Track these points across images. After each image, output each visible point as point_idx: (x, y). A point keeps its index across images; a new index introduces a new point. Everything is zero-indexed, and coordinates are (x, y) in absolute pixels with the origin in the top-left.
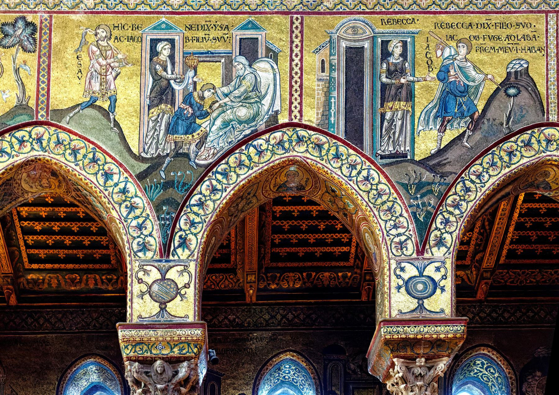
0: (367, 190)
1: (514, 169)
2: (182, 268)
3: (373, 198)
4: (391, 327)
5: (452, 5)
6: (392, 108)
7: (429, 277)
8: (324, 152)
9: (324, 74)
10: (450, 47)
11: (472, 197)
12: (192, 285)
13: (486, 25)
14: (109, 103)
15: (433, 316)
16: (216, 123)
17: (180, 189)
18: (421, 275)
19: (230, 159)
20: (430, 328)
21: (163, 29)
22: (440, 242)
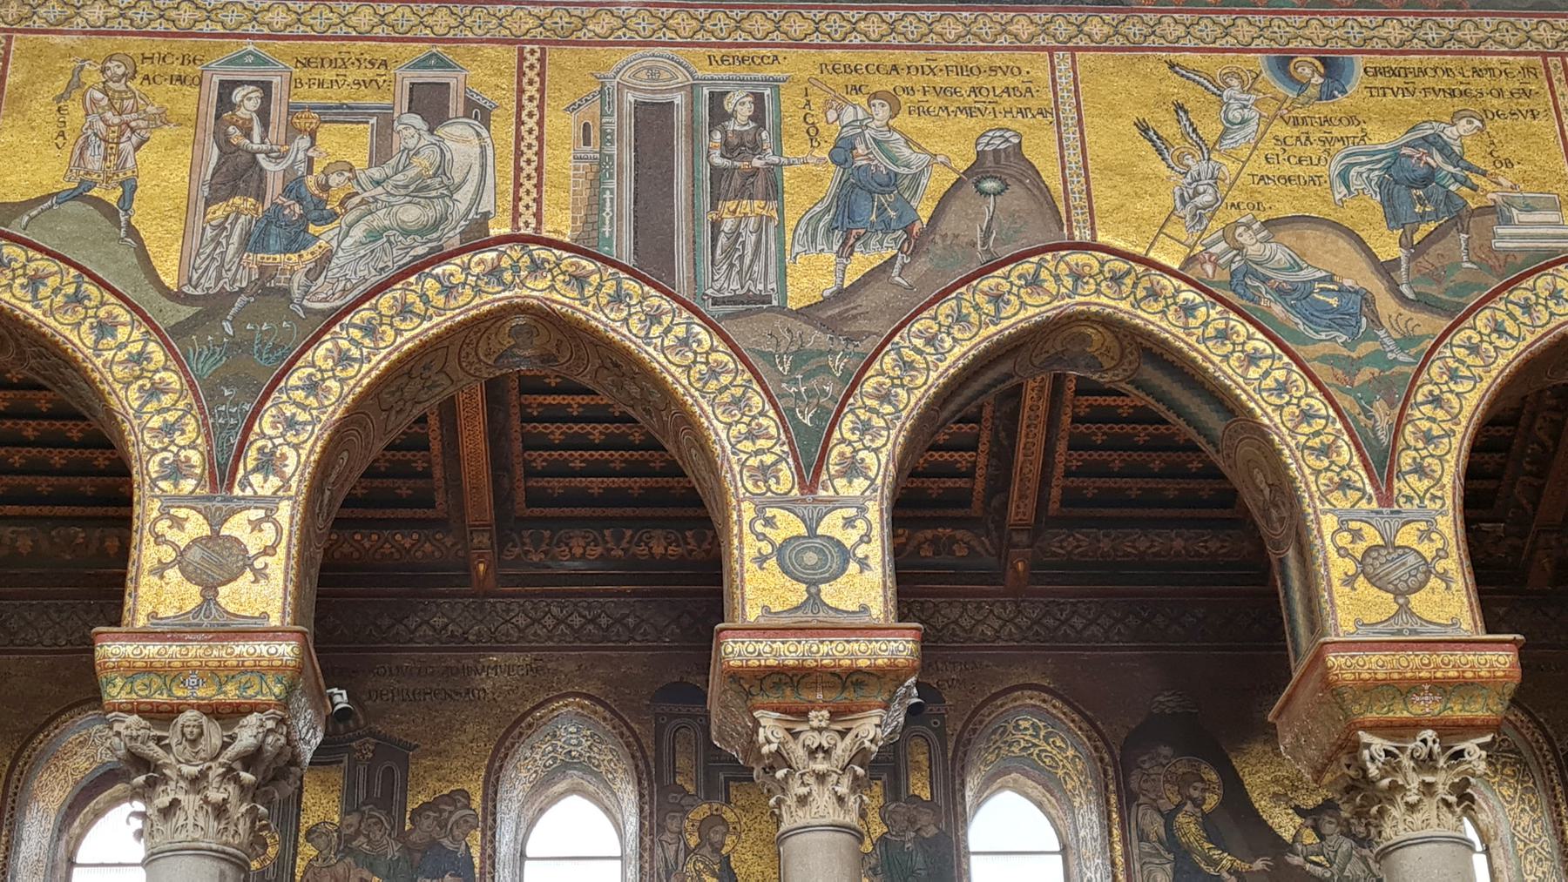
0: (687, 363)
1: (1007, 329)
2: (261, 513)
3: (700, 379)
4: (743, 643)
5: (855, 33)
6: (734, 212)
7: (830, 538)
8: (589, 290)
9: (588, 148)
10: (854, 107)
11: (920, 381)
12: (281, 551)
13: (926, 69)
14: (119, 191)
15: (845, 621)
16: (351, 233)
17: (265, 356)
18: (812, 533)
19: (381, 301)
20: (834, 645)
21: (248, 64)
22: (852, 469)
